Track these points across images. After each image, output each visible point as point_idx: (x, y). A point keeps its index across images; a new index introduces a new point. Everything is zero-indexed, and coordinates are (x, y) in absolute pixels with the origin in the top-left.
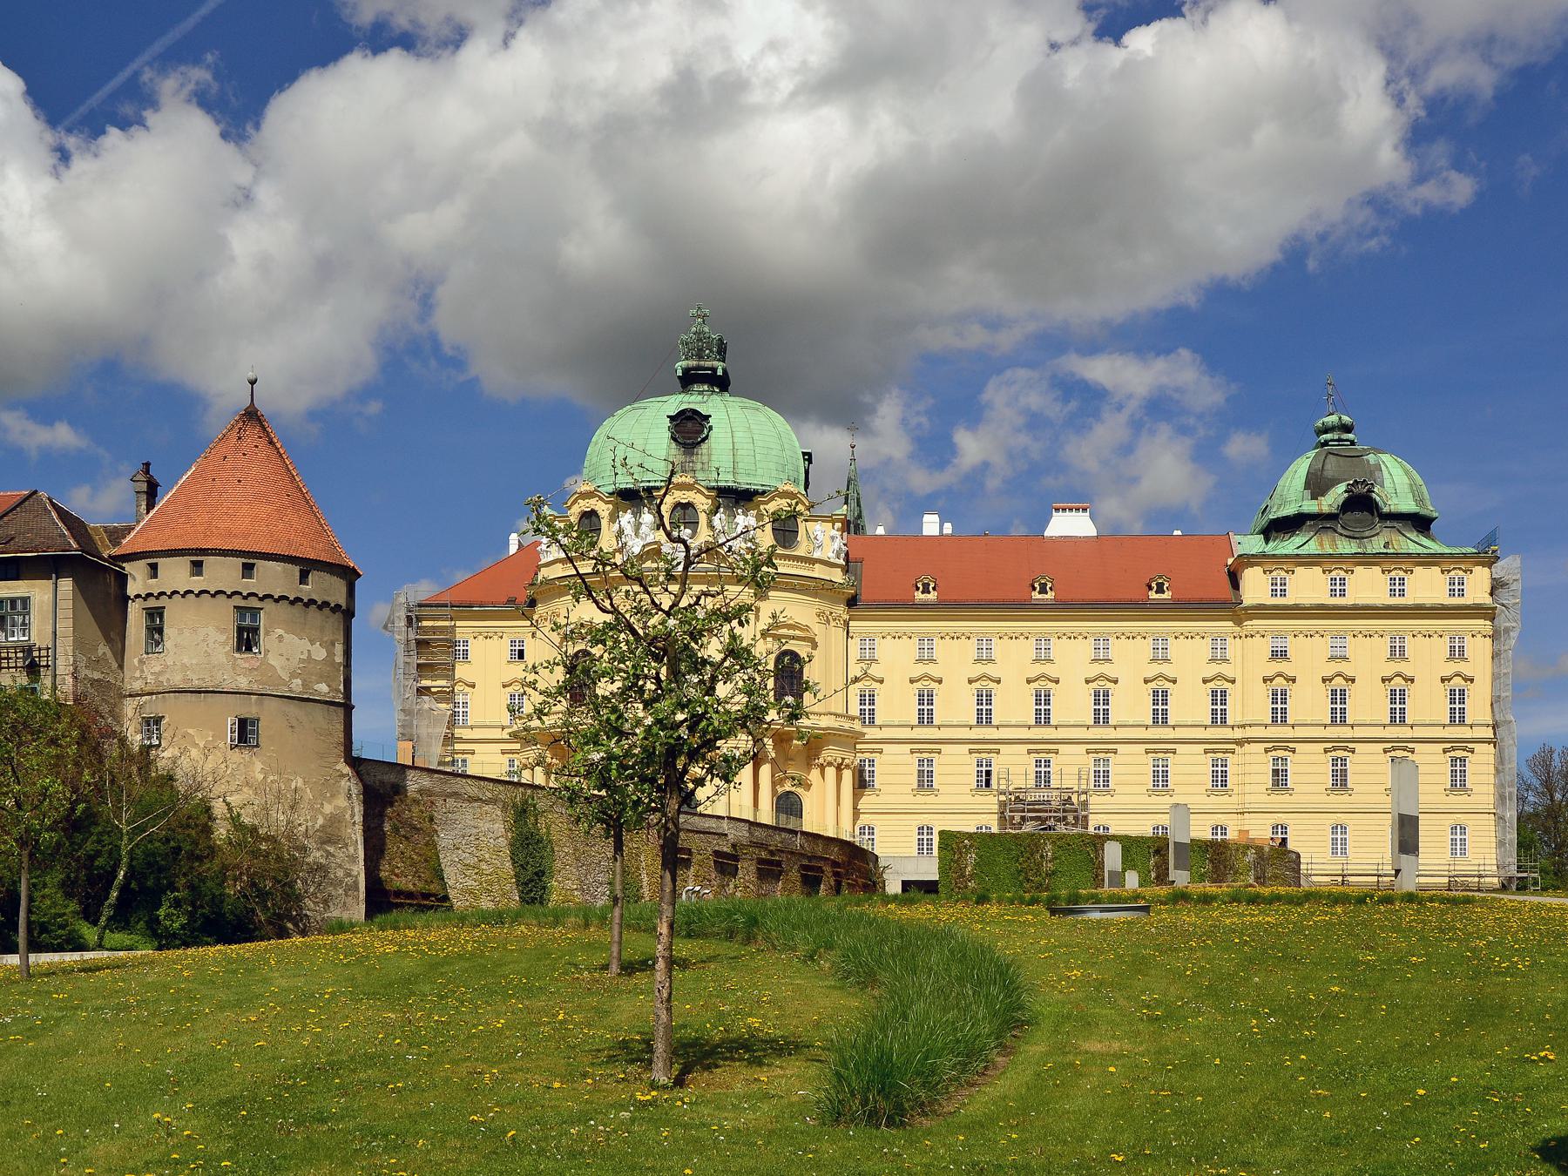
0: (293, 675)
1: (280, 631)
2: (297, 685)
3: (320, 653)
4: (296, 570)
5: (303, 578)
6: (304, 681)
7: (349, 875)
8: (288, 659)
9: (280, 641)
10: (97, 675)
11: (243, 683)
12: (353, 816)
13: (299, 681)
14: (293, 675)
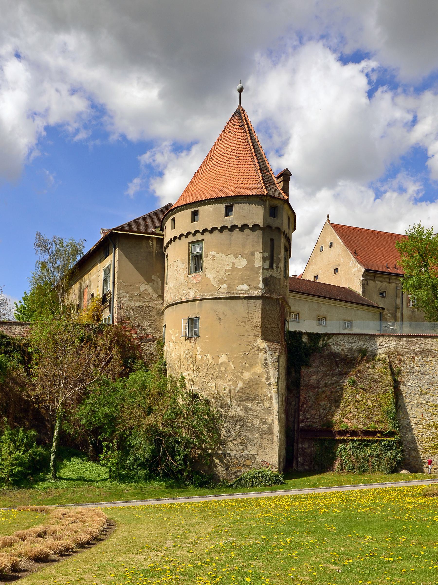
0: (221, 282)
1: (213, 253)
2: (224, 290)
3: (242, 263)
4: (222, 207)
5: (228, 210)
6: (229, 285)
7: (264, 422)
8: (218, 272)
9: (213, 260)
10: (138, 304)
11: (192, 294)
12: (268, 379)
13: (225, 286)
14: (221, 282)
